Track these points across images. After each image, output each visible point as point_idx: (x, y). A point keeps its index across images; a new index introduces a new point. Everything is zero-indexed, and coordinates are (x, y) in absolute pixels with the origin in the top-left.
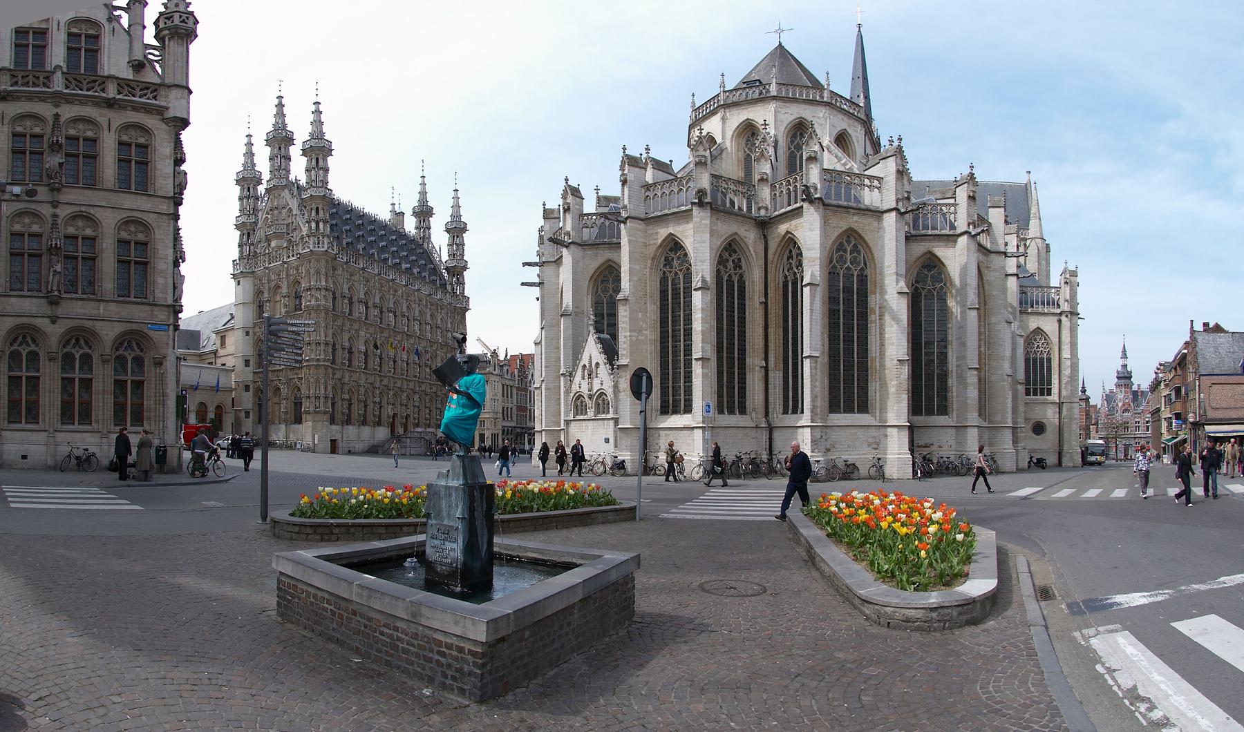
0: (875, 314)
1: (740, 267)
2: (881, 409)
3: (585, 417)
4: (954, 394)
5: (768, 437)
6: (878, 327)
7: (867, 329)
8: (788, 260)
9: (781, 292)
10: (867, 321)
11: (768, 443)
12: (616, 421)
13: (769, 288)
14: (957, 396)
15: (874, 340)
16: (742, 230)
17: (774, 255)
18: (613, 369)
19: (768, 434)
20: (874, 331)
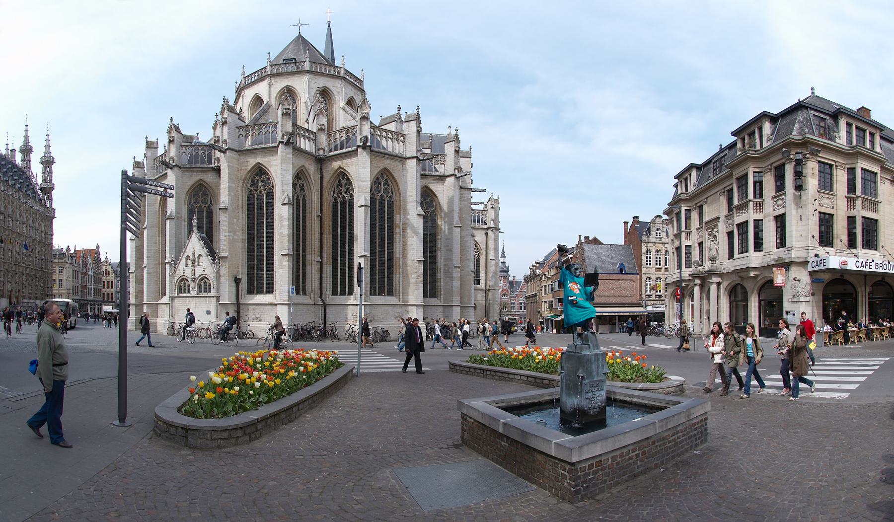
0: (399, 228)
1: (303, 190)
2: (403, 293)
3: (188, 295)
4: (442, 284)
5: (323, 311)
7: (393, 238)
8: (337, 187)
9: (331, 209)
11: (323, 316)
12: (218, 298)
13: (323, 206)
14: (444, 286)
16: (308, 164)
17: (328, 183)
18: (214, 260)
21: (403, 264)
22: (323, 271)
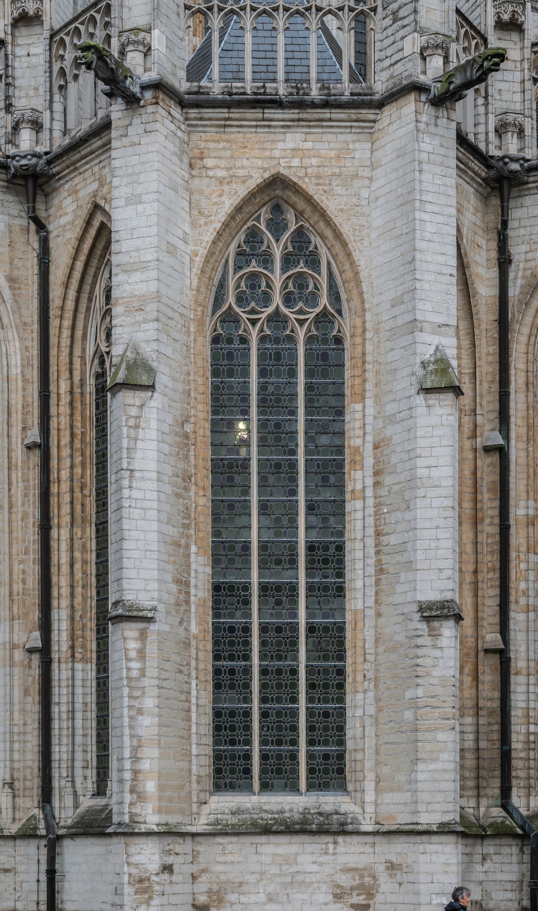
2: (378, 781)
6: (370, 511)
10: (341, 488)
15: (359, 554)
17: (67, 286)
19: (44, 859)
20: (359, 525)
21: (377, 641)
22: (55, 691)
